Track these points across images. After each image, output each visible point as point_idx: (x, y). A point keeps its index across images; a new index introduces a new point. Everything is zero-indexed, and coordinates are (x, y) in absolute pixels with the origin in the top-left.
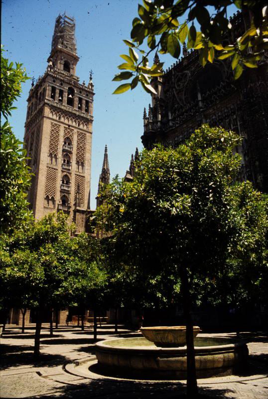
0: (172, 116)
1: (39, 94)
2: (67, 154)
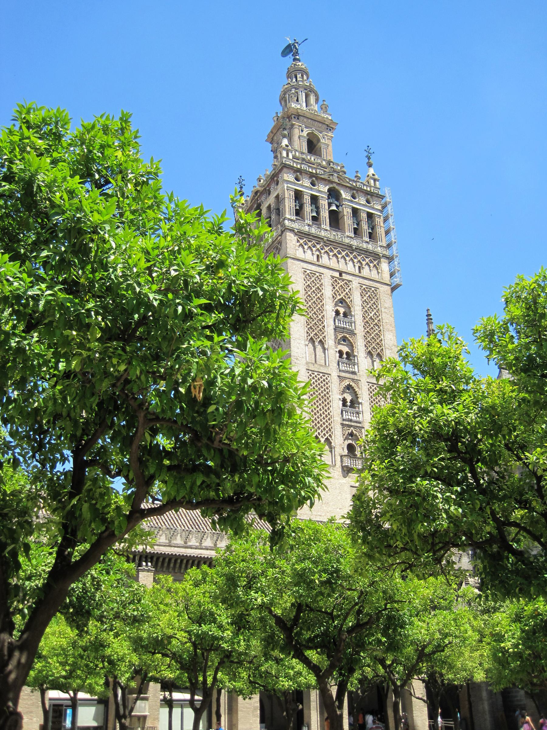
2: (345, 337)
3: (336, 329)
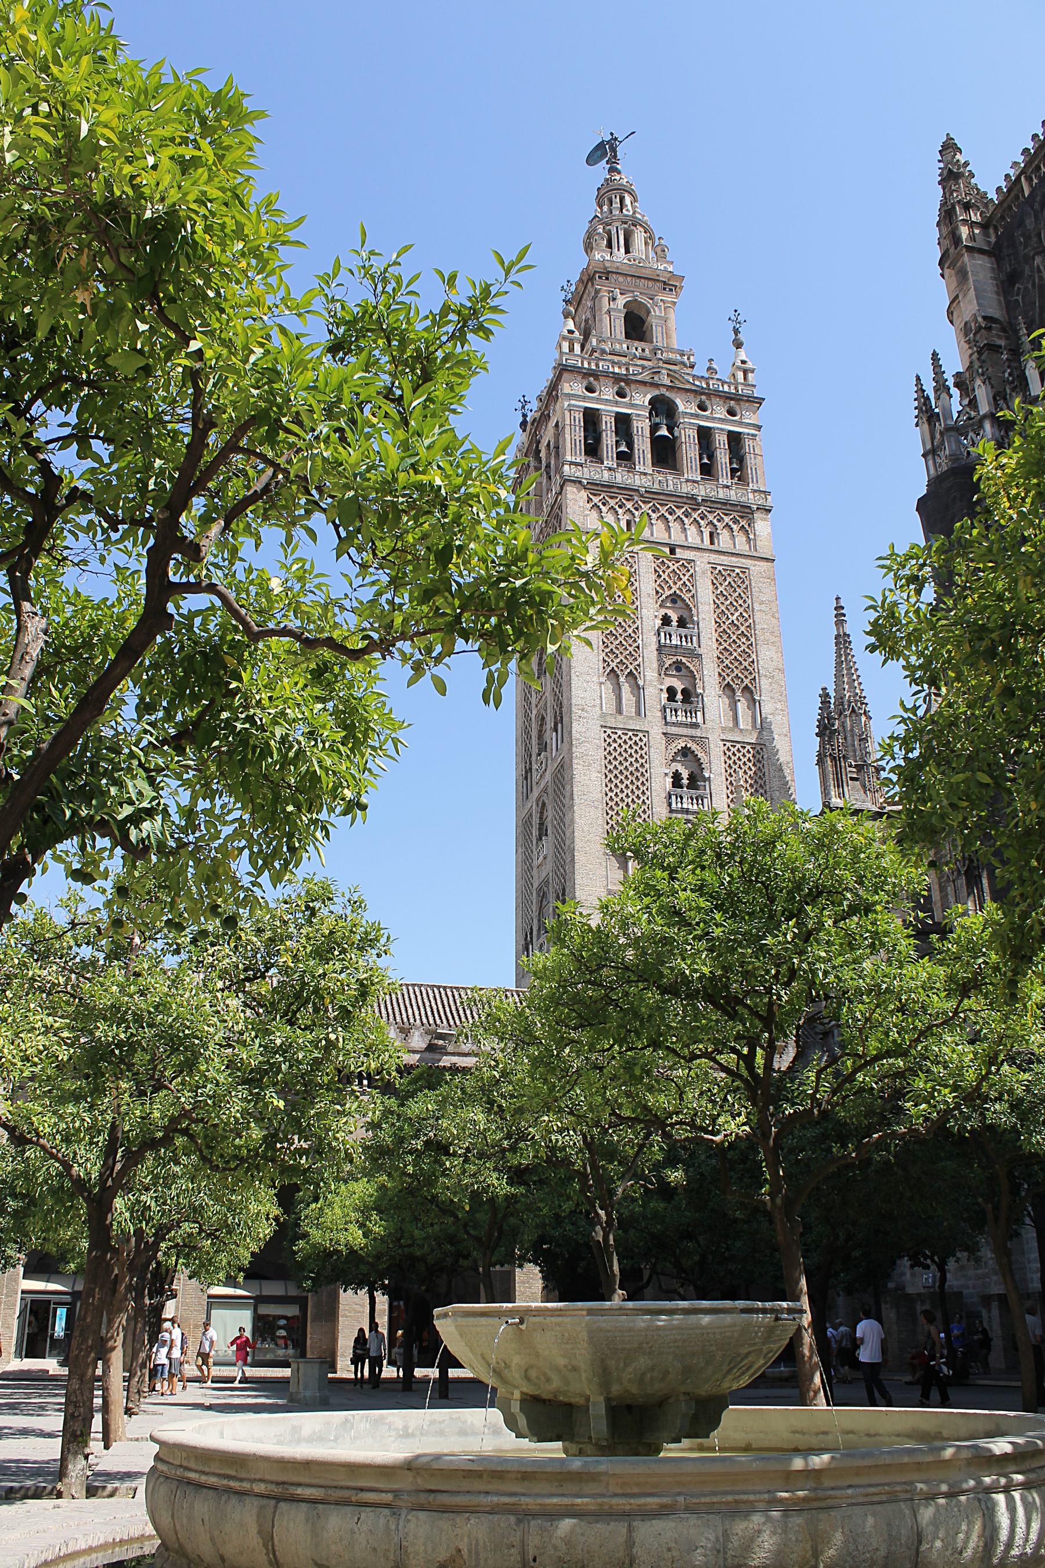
1: (543, 454)
2: (680, 663)
3: (660, 648)
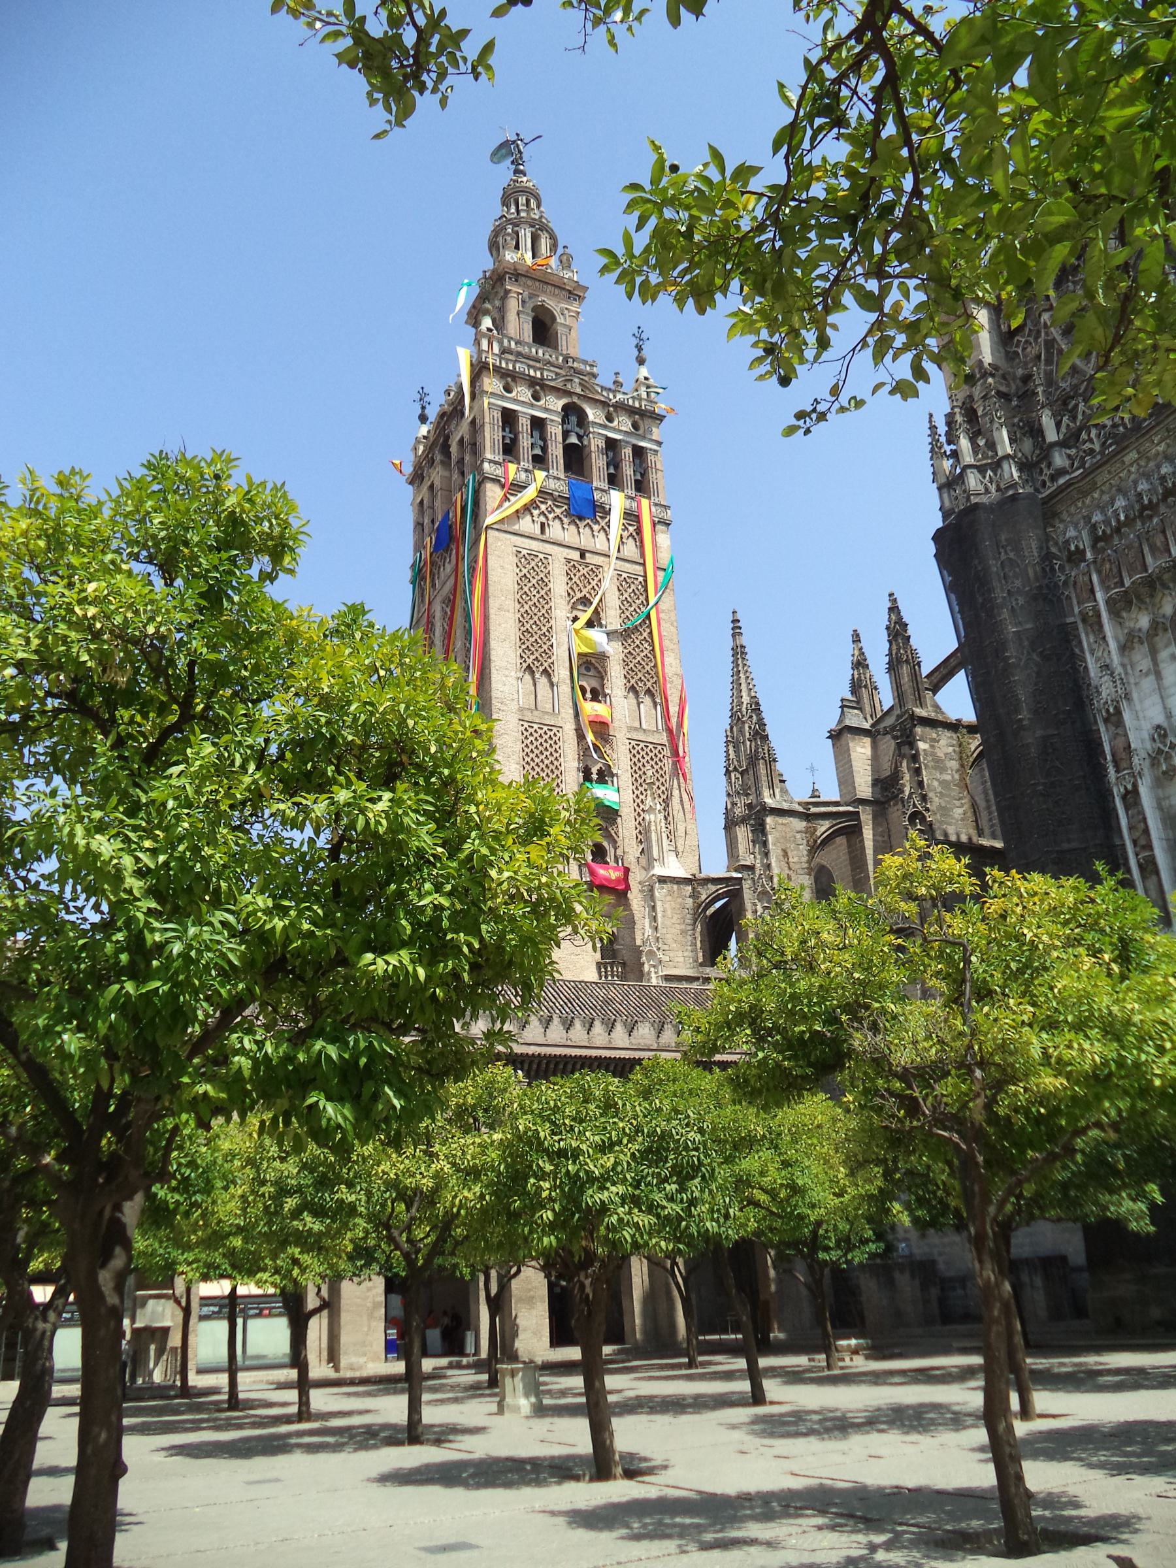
0: (1058, 425)
1: (454, 449)
